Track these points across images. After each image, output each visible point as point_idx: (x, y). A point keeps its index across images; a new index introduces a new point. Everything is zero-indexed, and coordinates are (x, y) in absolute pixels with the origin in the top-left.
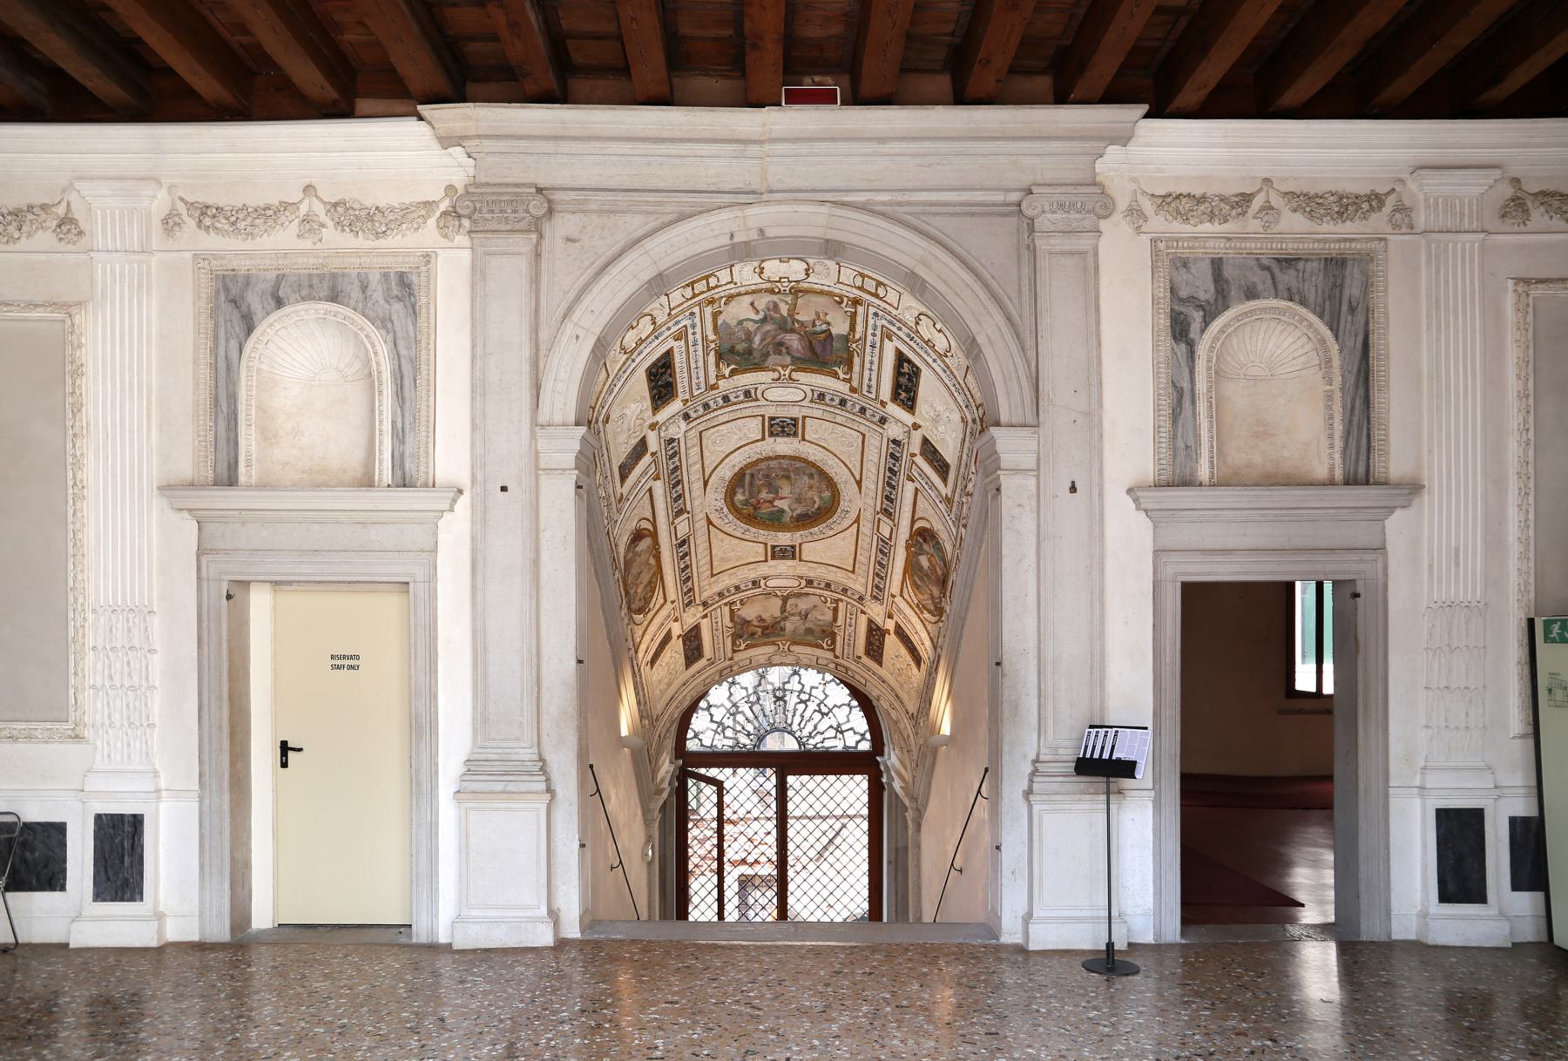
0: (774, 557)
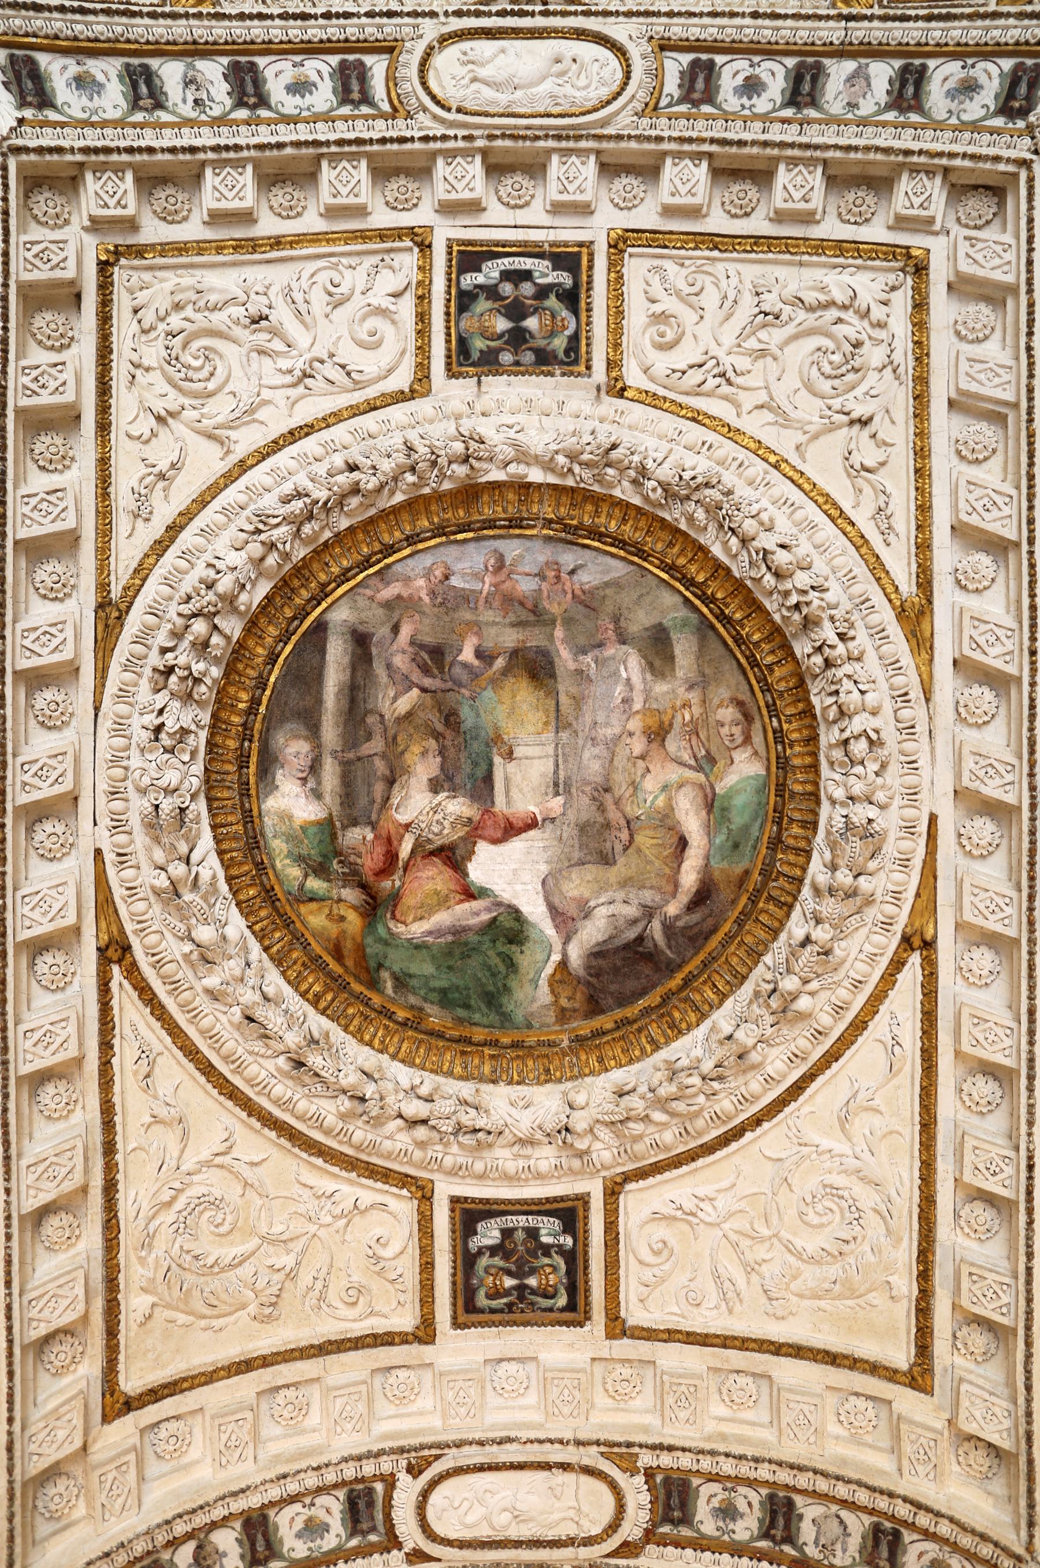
0: (468, 1310)
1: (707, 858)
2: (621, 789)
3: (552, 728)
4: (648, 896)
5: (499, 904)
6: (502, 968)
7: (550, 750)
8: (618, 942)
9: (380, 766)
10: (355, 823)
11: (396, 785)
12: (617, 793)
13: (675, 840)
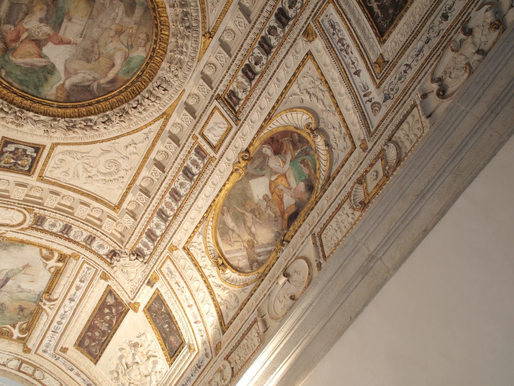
1: (119, 72)
2: (102, 42)
3: (87, 17)
4: (96, 75)
5: (49, 62)
6: (43, 79)
7: (84, 24)
8: (82, 84)
9: (24, 8)
10: (9, 23)
11: (28, 16)
12: (100, 44)
13: (112, 63)
